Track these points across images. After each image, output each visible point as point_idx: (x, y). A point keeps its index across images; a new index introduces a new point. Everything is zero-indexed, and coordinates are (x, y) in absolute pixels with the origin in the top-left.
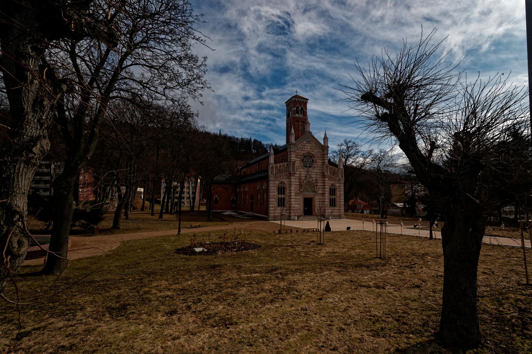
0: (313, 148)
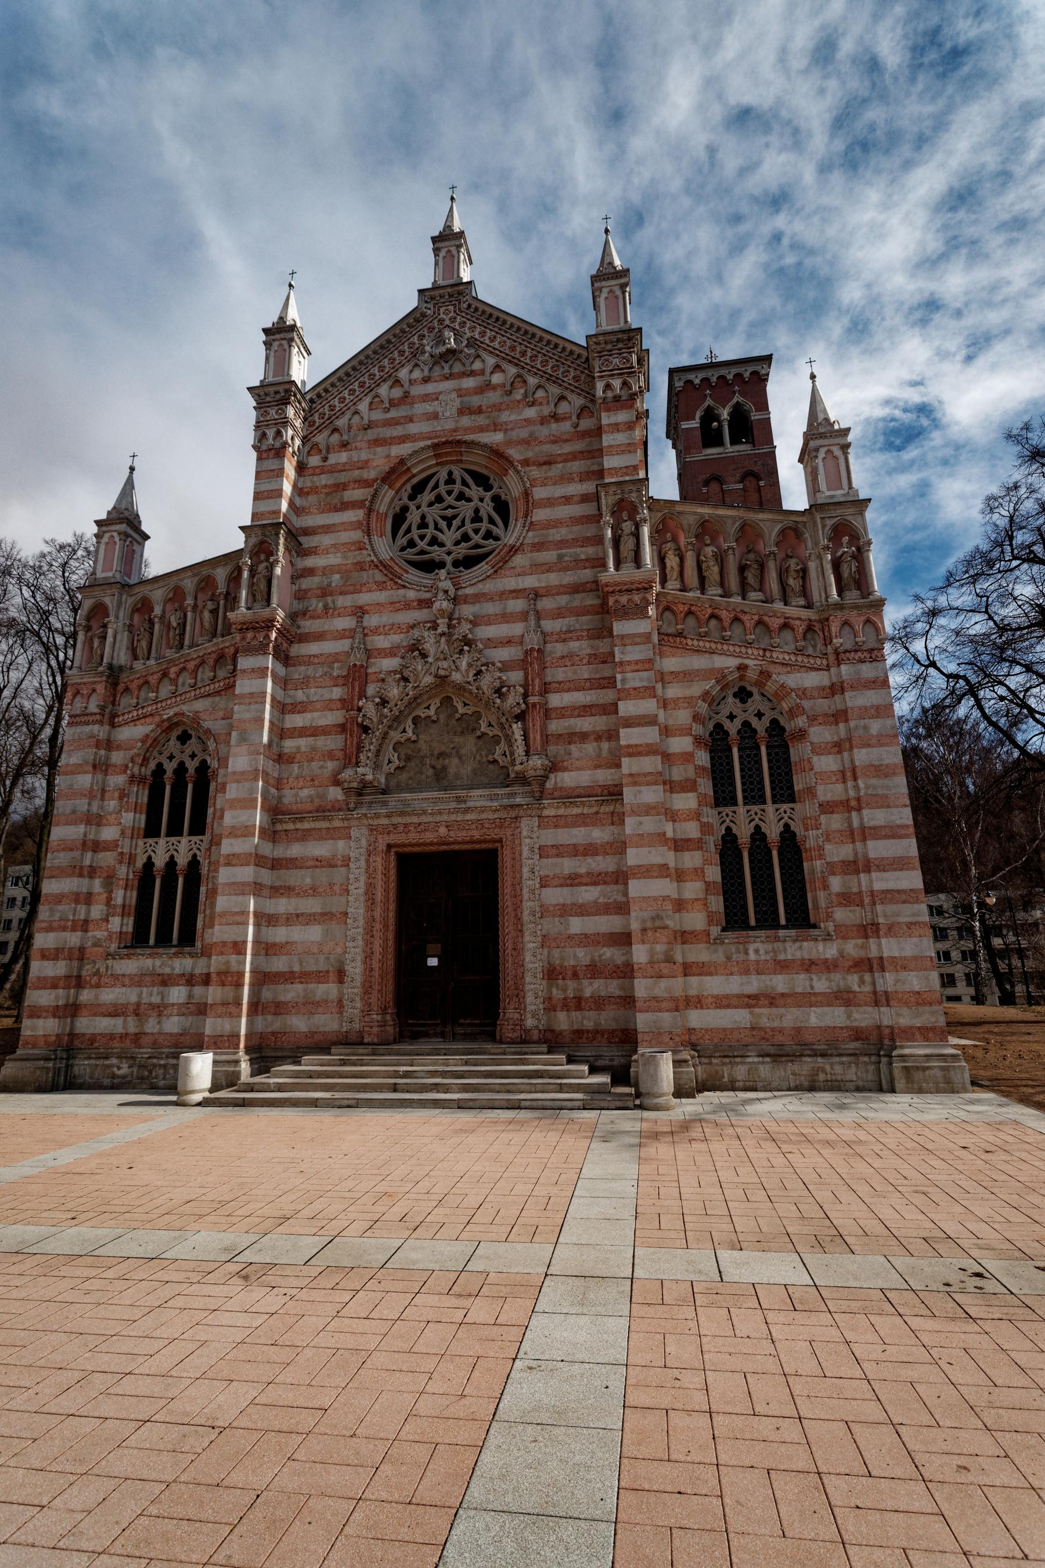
0: (493, 397)
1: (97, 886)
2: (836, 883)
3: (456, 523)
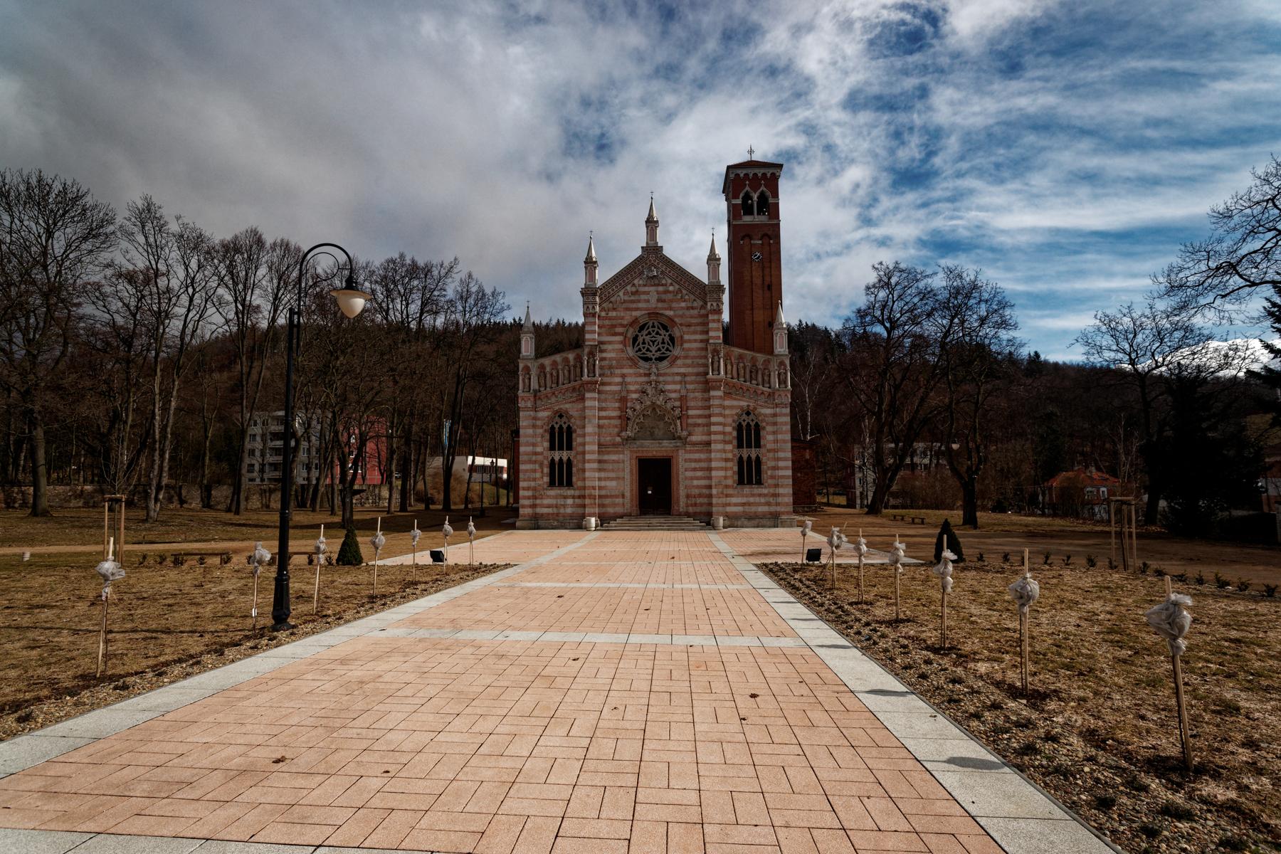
0: (670, 296)
1: (537, 467)
2: (769, 473)
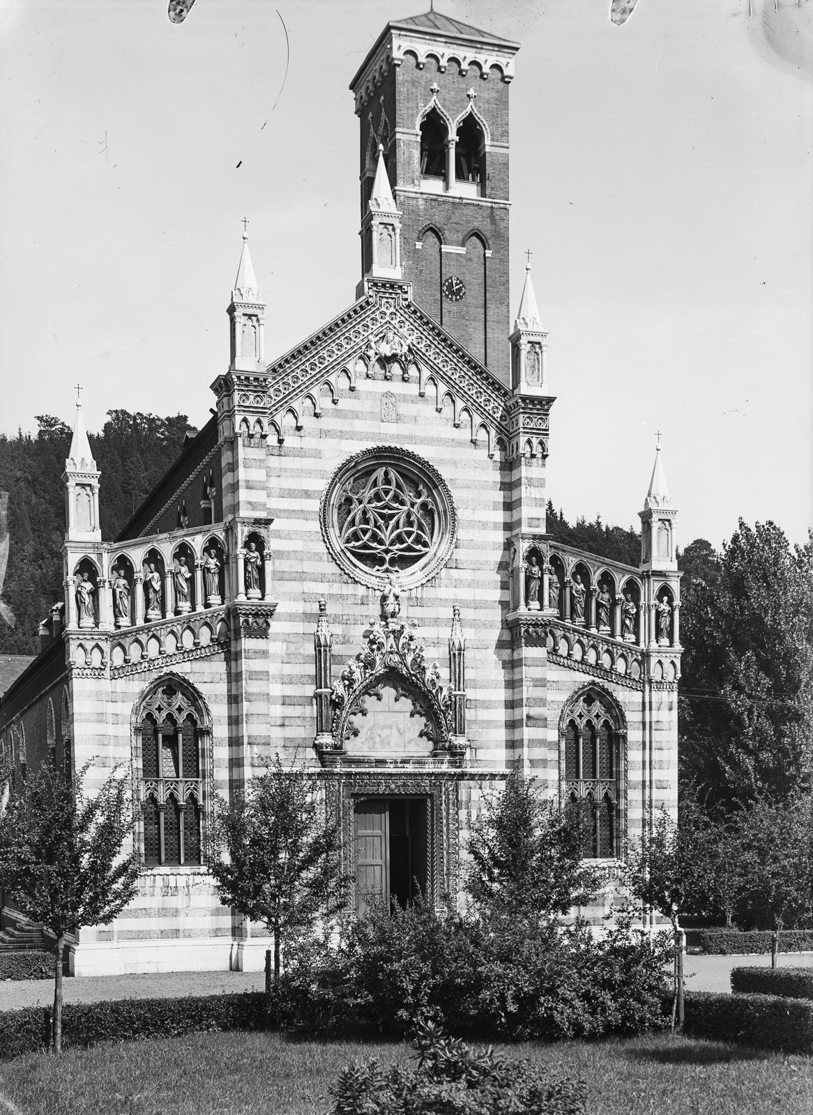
3: (392, 522)
